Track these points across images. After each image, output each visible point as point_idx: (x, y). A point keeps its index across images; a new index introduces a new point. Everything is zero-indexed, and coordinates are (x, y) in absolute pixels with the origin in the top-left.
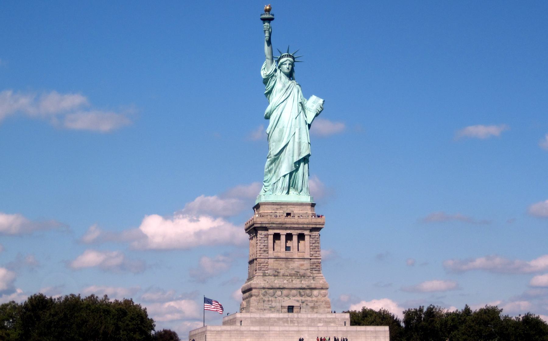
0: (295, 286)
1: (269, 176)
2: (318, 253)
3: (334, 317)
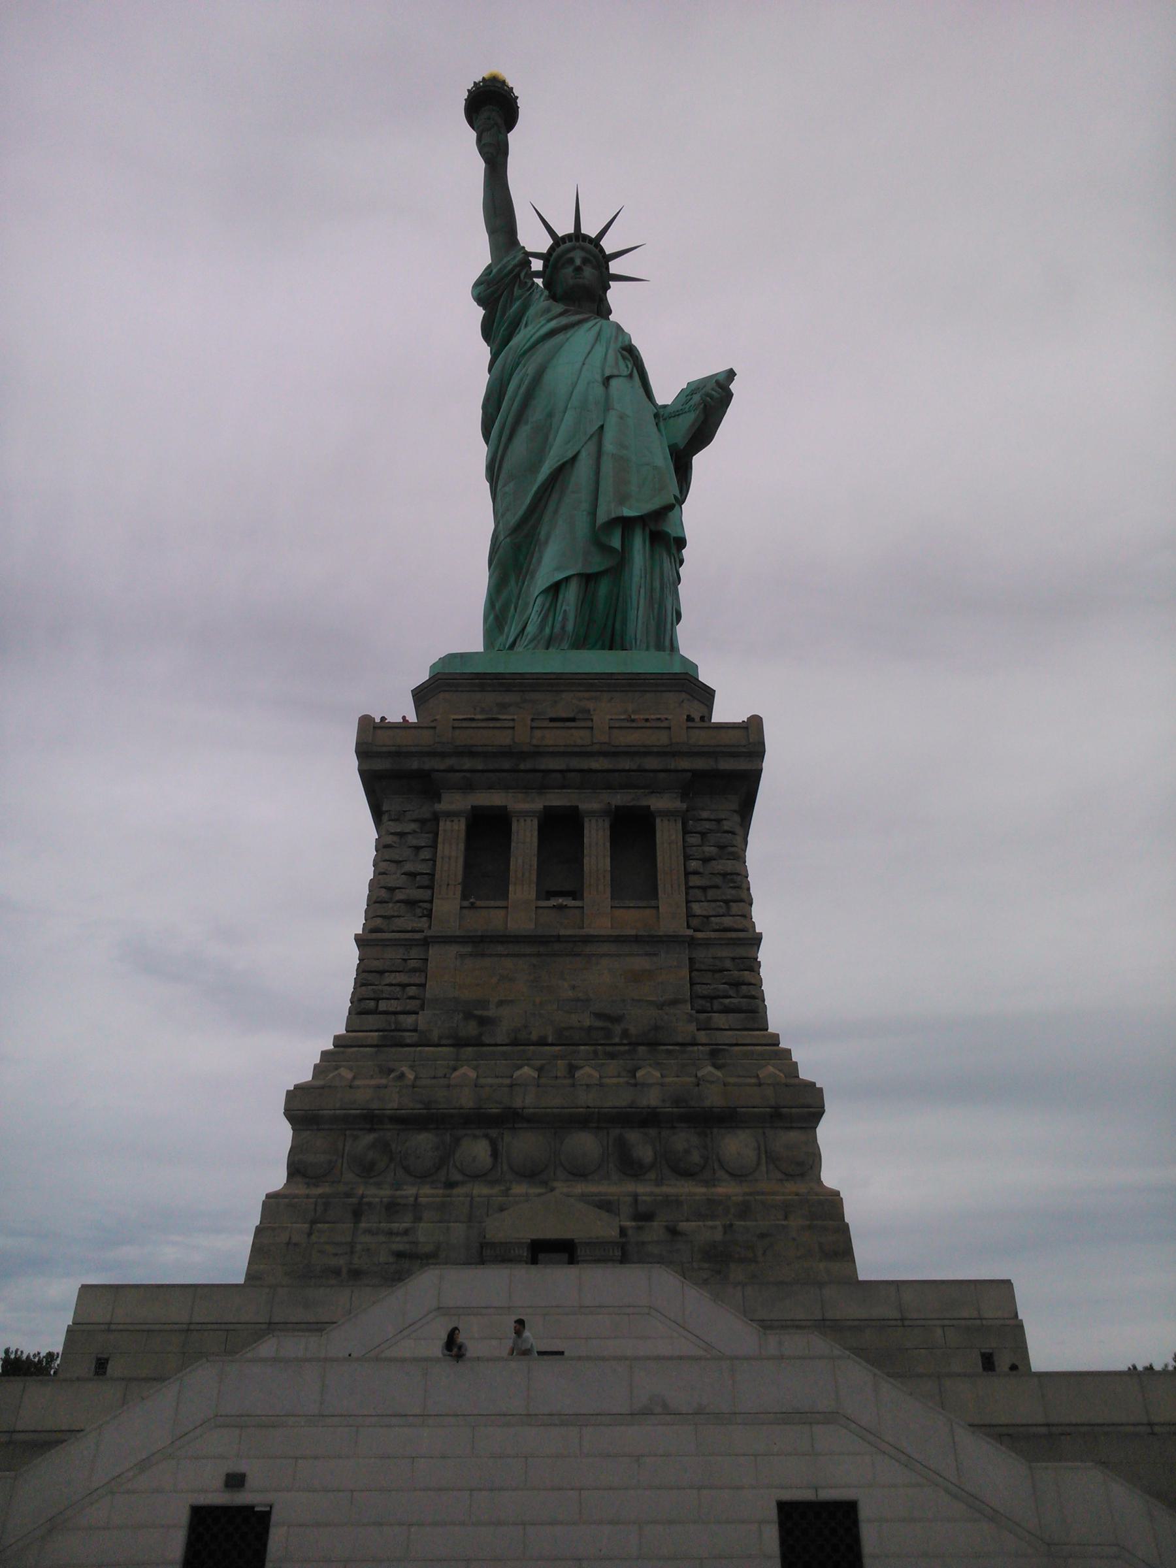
0: (586, 1099)
1: (502, 639)
2: (735, 909)
3: (898, 1316)
